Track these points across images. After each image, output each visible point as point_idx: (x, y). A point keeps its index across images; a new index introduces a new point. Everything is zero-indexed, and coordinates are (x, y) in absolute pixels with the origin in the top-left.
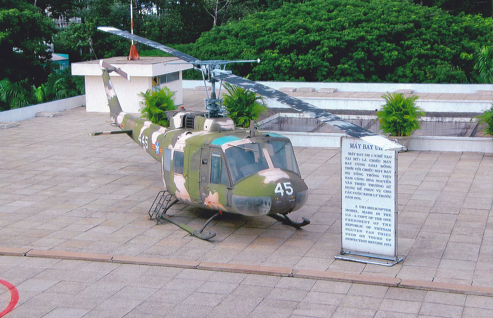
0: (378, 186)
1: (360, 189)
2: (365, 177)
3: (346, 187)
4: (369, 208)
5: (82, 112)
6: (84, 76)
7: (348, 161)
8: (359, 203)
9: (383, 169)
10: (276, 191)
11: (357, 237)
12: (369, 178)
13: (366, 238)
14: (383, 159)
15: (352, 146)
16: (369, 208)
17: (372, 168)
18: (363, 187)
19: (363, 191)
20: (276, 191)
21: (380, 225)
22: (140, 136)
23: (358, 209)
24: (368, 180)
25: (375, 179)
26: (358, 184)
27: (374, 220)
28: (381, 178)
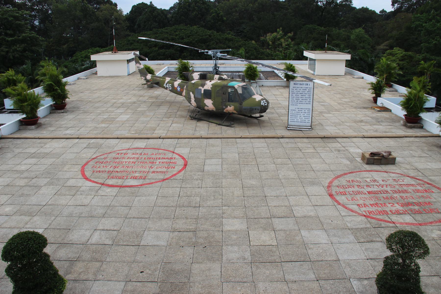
2: (300, 96)
5: (96, 76)
6: (96, 61)
8: (296, 107)
10: (262, 104)
11: (295, 120)
13: (299, 121)
15: (295, 84)
18: (299, 101)
19: (299, 102)
20: (262, 104)
21: (306, 115)
23: (297, 110)
25: (304, 97)
27: (303, 113)
28: (307, 96)
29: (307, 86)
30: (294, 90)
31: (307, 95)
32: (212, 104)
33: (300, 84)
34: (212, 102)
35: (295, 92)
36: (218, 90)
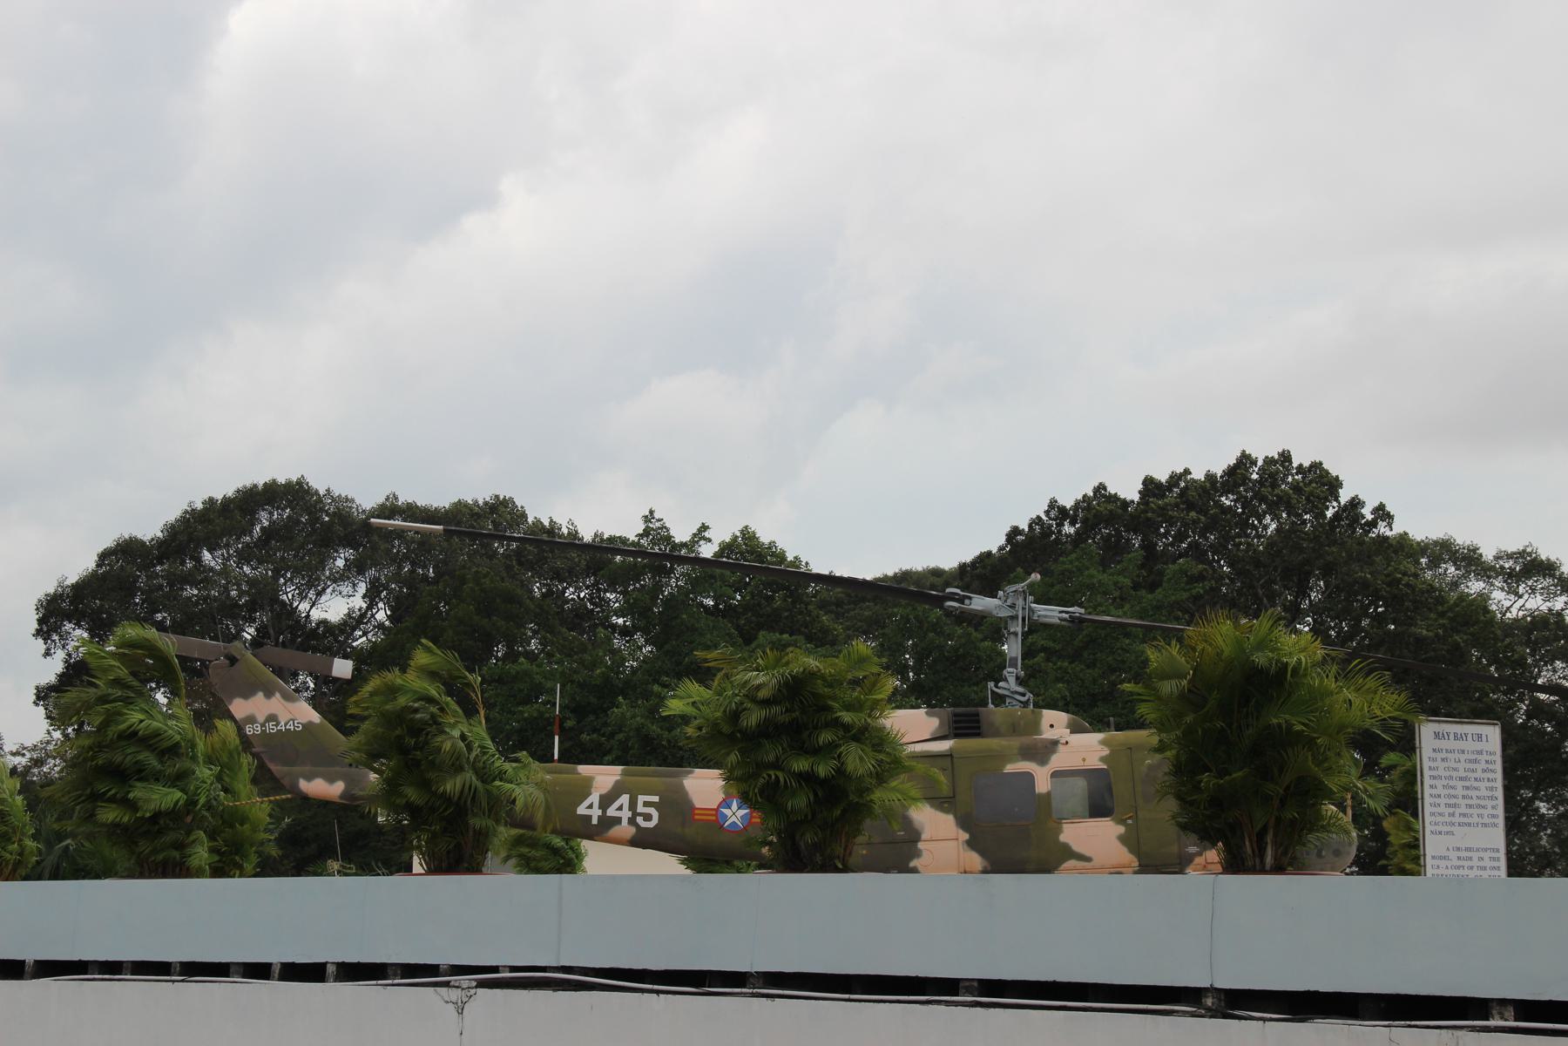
0: (1479, 806)
1: (1453, 815)
2: (1460, 792)
3: (1433, 814)
4: (1467, 849)
7: (1432, 764)
9: (1486, 775)
12: (1465, 793)
14: (1485, 757)
16: (1467, 849)
17: (1470, 775)
18: (1458, 811)
22: (594, 798)
23: (1453, 855)
24: (1464, 797)
25: (1474, 793)
26: (1449, 806)
29: (1478, 746)
30: (1439, 763)
31: (1482, 785)
32: (1123, 839)
33: (1456, 738)
34: (1121, 829)
35: (1441, 772)
36: (1150, 767)
